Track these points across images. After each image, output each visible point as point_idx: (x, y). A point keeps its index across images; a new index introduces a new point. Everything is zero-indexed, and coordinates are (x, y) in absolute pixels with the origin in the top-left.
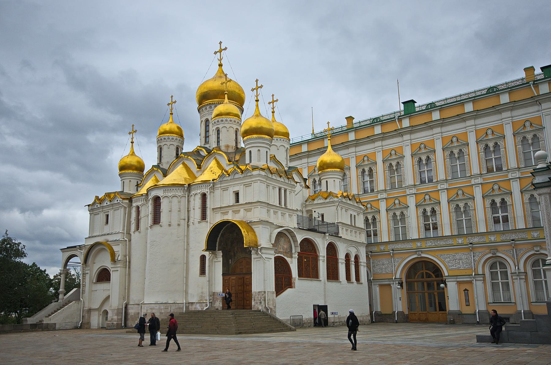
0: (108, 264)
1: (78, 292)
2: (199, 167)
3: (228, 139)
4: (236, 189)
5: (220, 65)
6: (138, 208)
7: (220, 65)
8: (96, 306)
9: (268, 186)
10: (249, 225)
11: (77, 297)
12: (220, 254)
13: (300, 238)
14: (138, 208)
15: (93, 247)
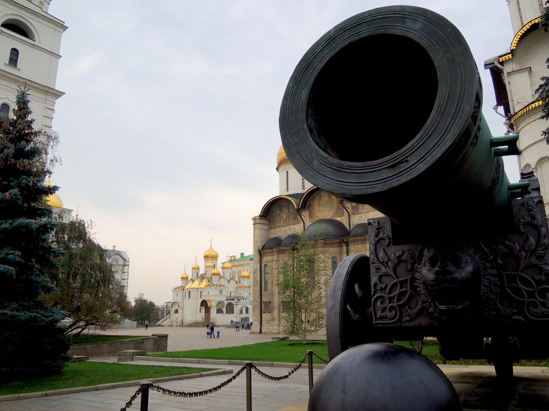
0: (178, 308)
1: (169, 316)
2: (201, 282)
3: (209, 275)
4: (208, 291)
5: (211, 245)
6: (185, 292)
7: (211, 245)
8: (175, 320)
9: (216, 290)
10: (210, 301)
11: (169, 317)
12: (204, 307)
13: (226, 303)
14: (185, 292)
15: (173, 303)
